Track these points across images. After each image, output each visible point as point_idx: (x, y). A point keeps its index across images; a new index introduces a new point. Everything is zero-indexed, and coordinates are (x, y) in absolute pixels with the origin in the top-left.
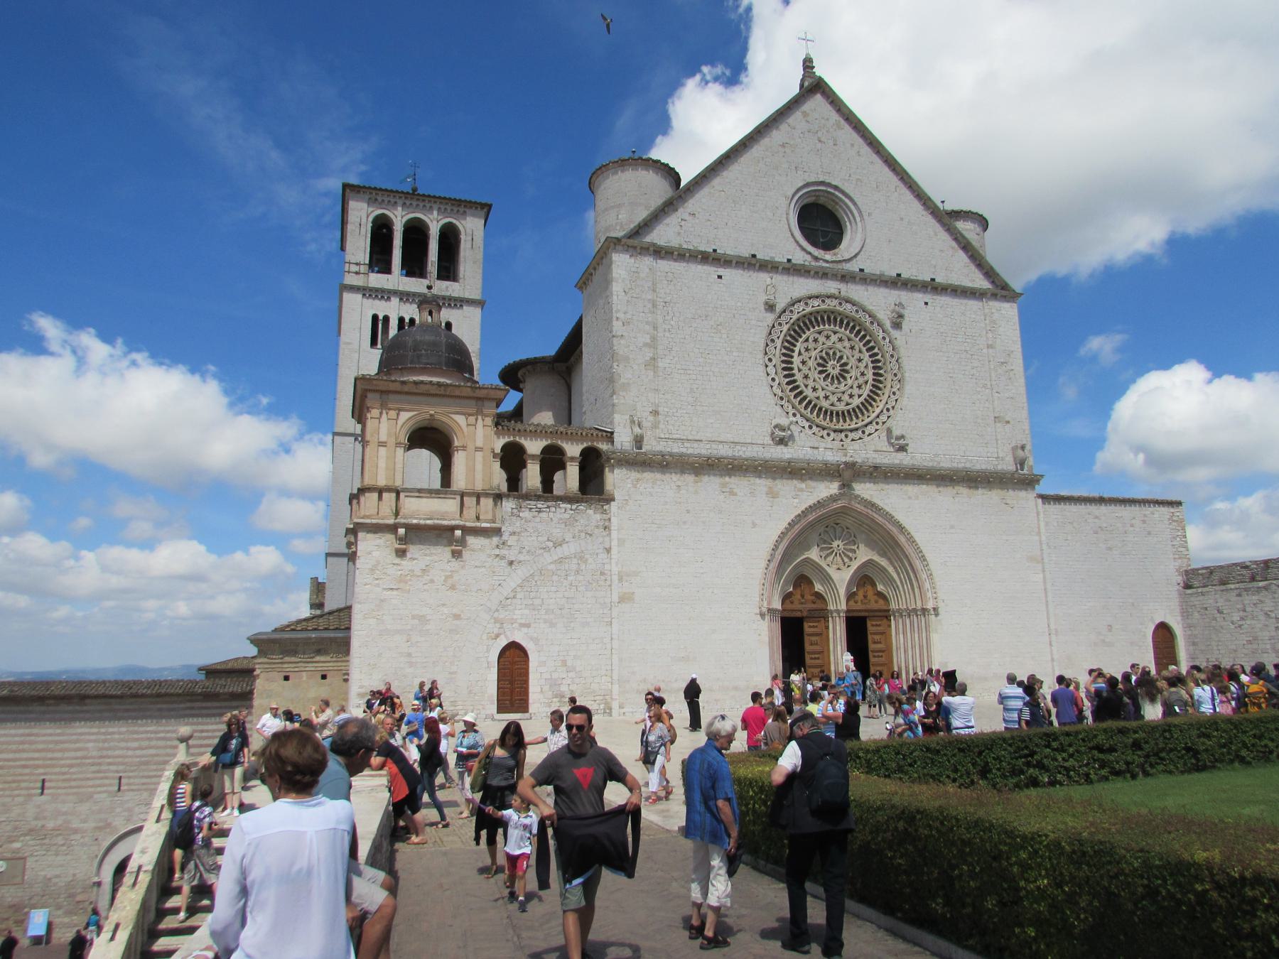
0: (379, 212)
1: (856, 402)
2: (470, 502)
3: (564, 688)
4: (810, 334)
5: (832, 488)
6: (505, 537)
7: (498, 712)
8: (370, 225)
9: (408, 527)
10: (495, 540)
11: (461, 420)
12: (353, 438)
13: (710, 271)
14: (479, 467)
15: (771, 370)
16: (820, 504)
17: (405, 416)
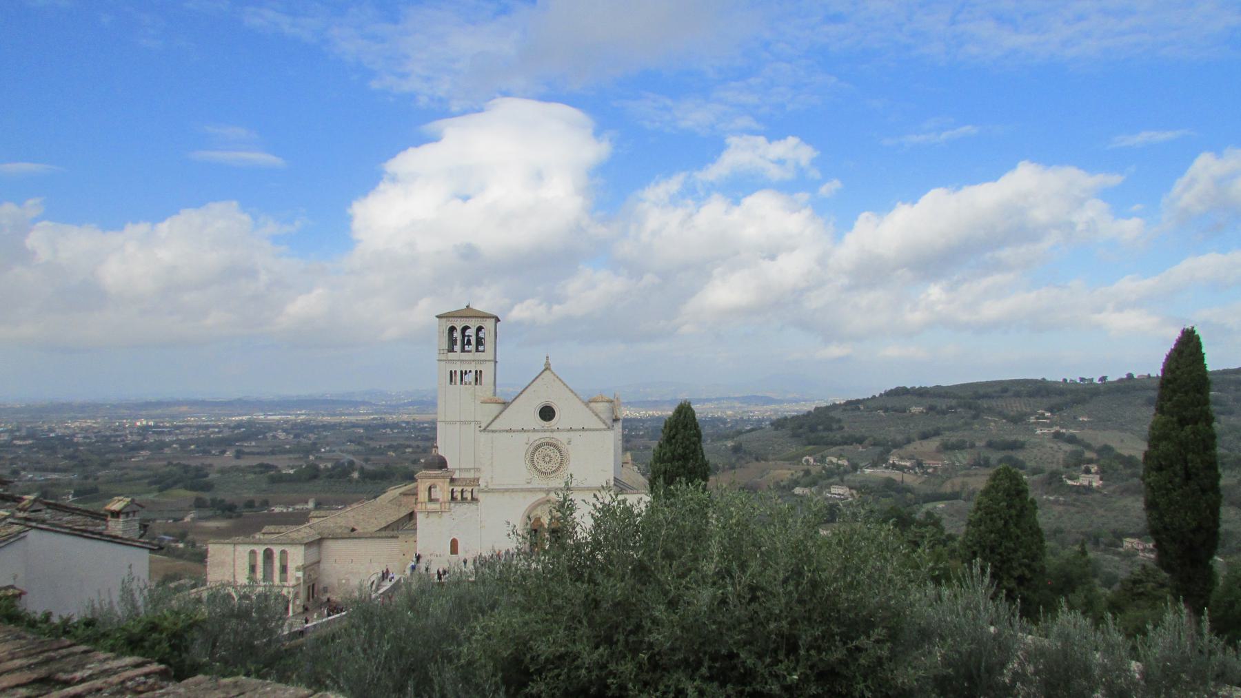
0: (451, 325)
1: (554, 469)
2: (443, 504)
3: (467, 549)
4: (541, 449)
5: (544, 495)
6: (452, 512)
7: (451, 554)
8: (447, 331)
9: (428, 512)
10: (449, 513)
11: (441, 484)
12: (444, 424)
13: (510, 434)
14: (446, 496)
15: (527, 462)
16: (539, 500)
17: (427, 484)
